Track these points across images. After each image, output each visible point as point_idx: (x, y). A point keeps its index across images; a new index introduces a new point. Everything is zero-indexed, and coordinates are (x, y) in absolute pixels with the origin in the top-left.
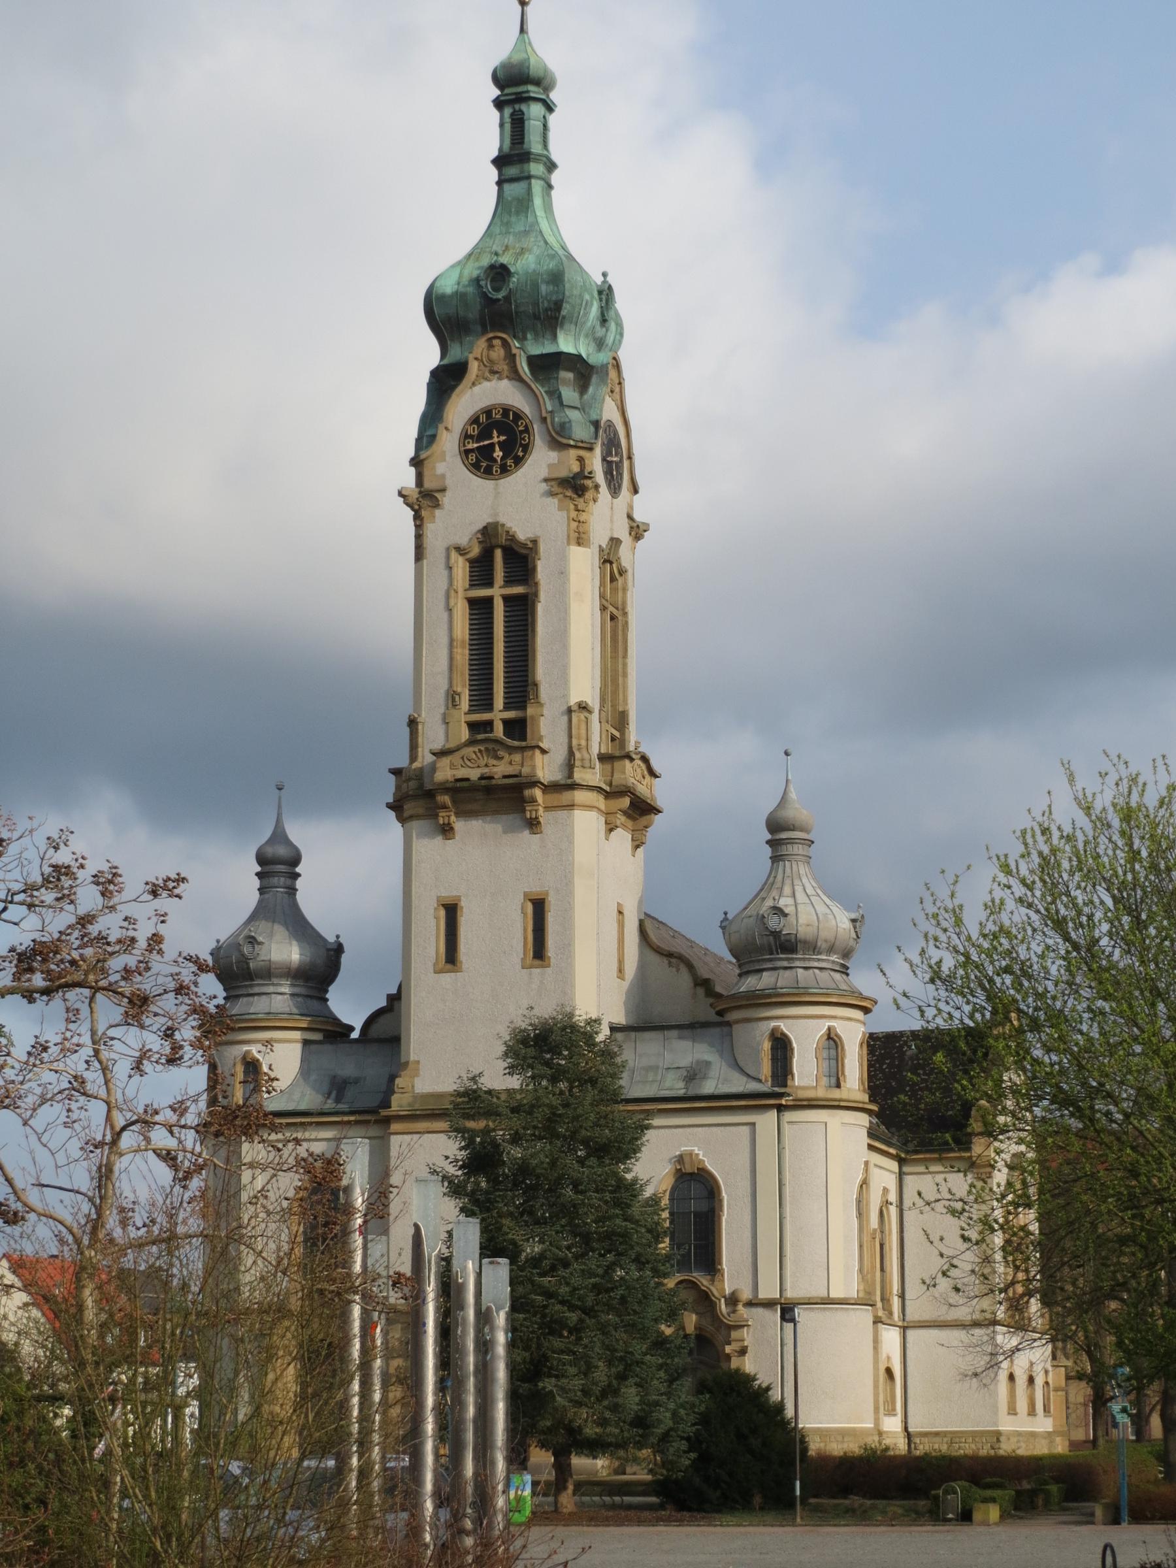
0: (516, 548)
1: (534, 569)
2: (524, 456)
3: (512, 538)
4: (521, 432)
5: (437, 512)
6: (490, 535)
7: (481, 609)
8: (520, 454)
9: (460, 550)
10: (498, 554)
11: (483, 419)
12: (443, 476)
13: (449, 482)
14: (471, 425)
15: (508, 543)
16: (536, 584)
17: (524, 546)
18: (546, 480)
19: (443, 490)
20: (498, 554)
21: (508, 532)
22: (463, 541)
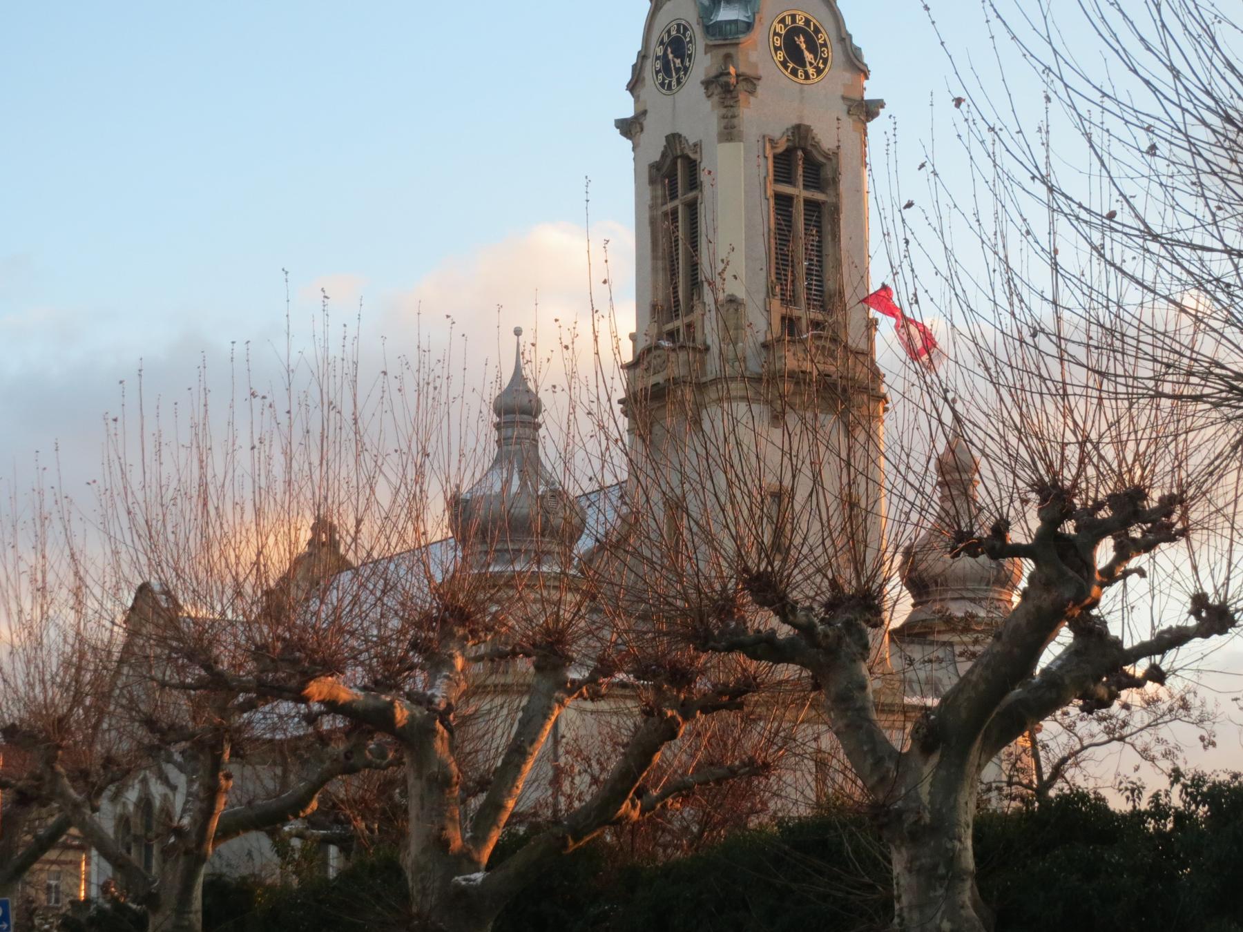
0: (815, 152)
1: (835, 182)
2: (824, 69)
3: (816, 145)
4: (822, 45)
5: (752, 99)
6: (800, 133)
7: (783, 203)
8: (821, 66)
9: (771, 141)
10: (800, 153)
11: (788, 20)
12: (755, 66)
13: (761, 72)
14: (779, 22)
15: (809, 148)
16: (838, 195)
17: (826, 156)
18: (844, 98)
19: (759, 79)
20: (800, 153)
21: (813, 138)
22: (776, 134)
